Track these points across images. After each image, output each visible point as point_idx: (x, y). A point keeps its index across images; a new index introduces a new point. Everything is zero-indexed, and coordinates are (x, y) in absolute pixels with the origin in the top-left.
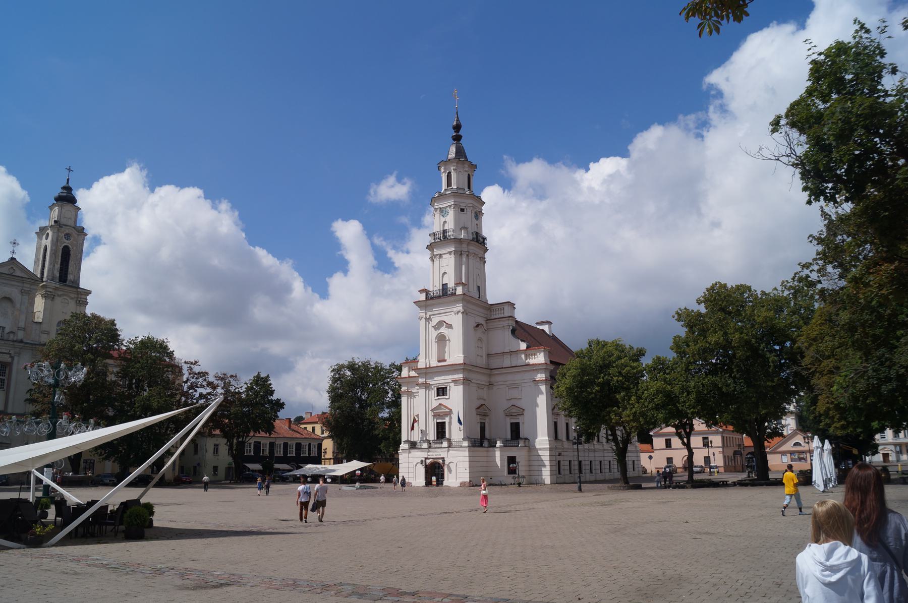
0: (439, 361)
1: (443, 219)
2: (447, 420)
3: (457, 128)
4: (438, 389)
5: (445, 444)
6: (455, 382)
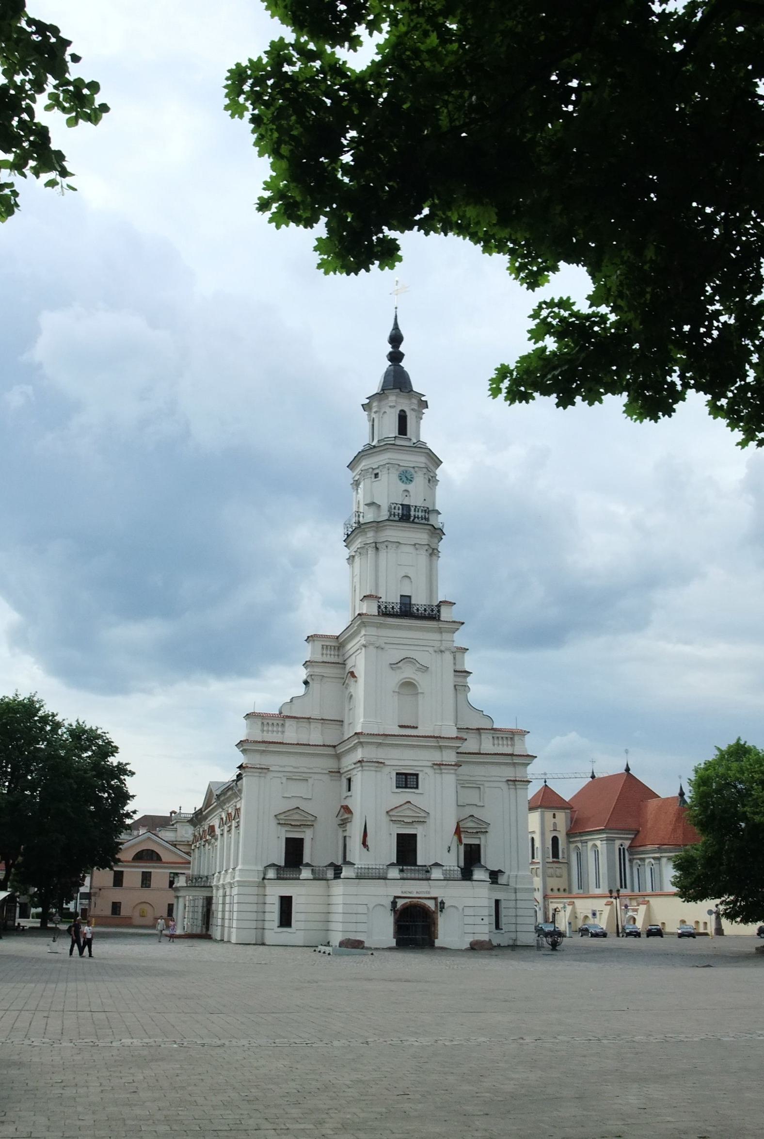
0: (400, 726)
1: (403, 486)
2: (418, 830)
3: (396, 339)
4: (397, 774)
5: (436, 874)
6: (439, 766)
